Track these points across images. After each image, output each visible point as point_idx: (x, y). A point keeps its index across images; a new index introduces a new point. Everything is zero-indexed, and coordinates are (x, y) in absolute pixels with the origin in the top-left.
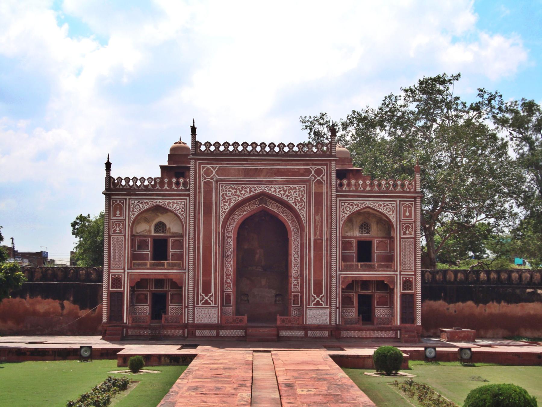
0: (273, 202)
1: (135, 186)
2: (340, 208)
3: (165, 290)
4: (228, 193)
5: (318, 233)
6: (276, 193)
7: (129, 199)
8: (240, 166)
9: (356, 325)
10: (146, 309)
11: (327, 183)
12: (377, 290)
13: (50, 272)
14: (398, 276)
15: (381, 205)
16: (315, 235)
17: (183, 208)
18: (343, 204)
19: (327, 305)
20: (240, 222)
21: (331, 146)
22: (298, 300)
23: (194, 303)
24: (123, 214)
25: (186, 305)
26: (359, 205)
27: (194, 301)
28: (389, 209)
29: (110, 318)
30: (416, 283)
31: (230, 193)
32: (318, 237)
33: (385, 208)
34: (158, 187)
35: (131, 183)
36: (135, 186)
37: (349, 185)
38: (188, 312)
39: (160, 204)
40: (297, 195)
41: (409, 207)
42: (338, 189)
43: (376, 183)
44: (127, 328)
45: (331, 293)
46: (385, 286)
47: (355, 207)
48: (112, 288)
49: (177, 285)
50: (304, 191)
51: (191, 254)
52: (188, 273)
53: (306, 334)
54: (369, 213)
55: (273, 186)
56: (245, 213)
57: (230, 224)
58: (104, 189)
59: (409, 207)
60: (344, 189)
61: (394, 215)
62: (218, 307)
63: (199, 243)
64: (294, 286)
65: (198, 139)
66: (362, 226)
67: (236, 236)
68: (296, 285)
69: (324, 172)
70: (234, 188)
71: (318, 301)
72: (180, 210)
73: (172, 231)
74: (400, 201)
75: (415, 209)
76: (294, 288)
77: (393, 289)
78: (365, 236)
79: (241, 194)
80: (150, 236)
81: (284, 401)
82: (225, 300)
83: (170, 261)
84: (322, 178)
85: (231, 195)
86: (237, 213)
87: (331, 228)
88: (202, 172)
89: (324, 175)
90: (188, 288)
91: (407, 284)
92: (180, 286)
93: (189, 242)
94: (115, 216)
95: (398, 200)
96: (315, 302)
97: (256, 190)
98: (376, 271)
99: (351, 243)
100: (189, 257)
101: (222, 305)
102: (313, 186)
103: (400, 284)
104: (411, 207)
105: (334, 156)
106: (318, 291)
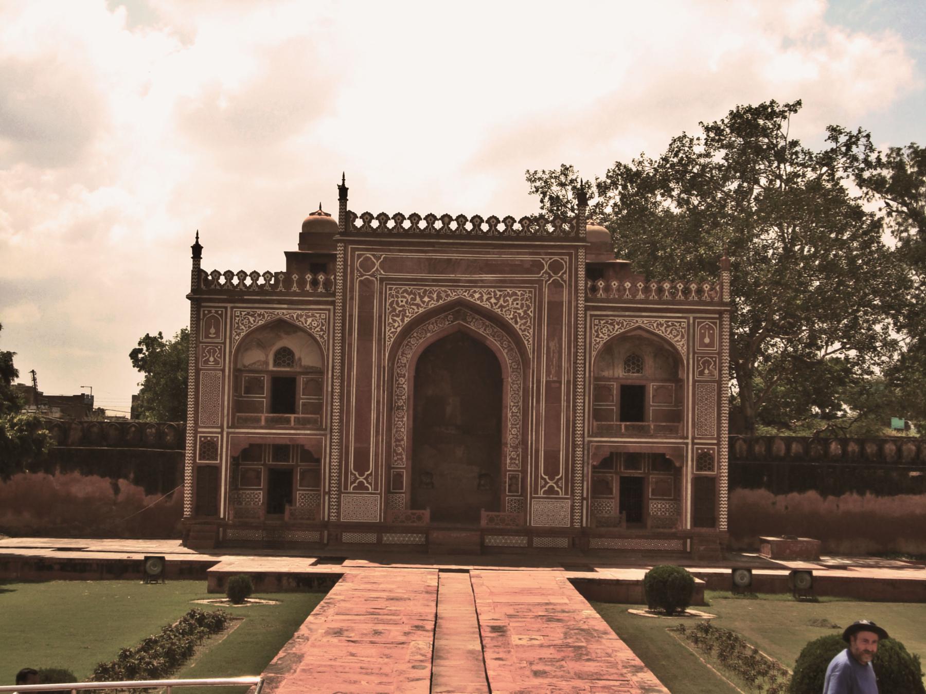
0: (477, 317)
1: (241, 286)
2: (591, 328)
3: (291, 463)
4: (400, 300)
6: (482, 301)
7: (232, 308)
8: (422, 255)
9: (616, 529)
10: (257, 496)
11: (570, 285)
12: (653, 470)
13: (95, 429)
14: (690, 447)
15: (662, 325)
16: (548, 373)
17: (323, 325)
18: (597, 322)
19: (566, 493)
20: (421, 350)
21: (577, 223)
22: (517, 485)
25: (327, 490)
27: (339, 483)
28: (673, 330)
29: (197, 508)
30: (719, 459)
31: (405, 300)
32: (553, 378)
33: (669, 330)
34: (281, 288)
35: (235, 281)
36: (241, 286)
37: (607, 289)
38: (329, 502)
40: (519, 306)
41: (711, 328)
42: (590, 295)
43: (654, 286)
44: (226, 526)
46: (666, 464)
47: (617, 327)
49: (312, 457)
50: (531, 298)
51: (337, 404)
52: (331, 436)
53: (530, 542)
54: (640, 338)
55: (477, 290)
56: (429, 335)
57: (403, 353)
58: (189, 291)
59: (711, 328)
60: (599, 296)
62: (380, 494)
63: (349, 385)
64: (510, 461)
65: (350, 207)
66: (629, 360)
67: (413, 373)
70: (411, 293)
71: (551, 487)
72: (318, 329)
74: (694, 318)
75: (721, 332)
76: (511, 463)
77: (681, 468)
78: (633, 378)
79: (424, 302)
81: (489, 655)
82: (394, 483)
83: (301, 416)
84: (561, 277)
85: (406, 305)
86: (415, 335)
87: (575, 363)
88: (357, 264)
89: (565, 273)
90: (330, 461)
91: (705, 460)
92: (316, 456)
93: (333, 382)
94: (207, 337)
95: (691, 316)
96: (546, 488)
97: (448, 296)
98: (651, 437)
99: (609, 389)
100: (332, 409)
101: (388, 491)
102: (546, 291)
104: (713, 329)
105: (583, 240)
106: (552, 470)
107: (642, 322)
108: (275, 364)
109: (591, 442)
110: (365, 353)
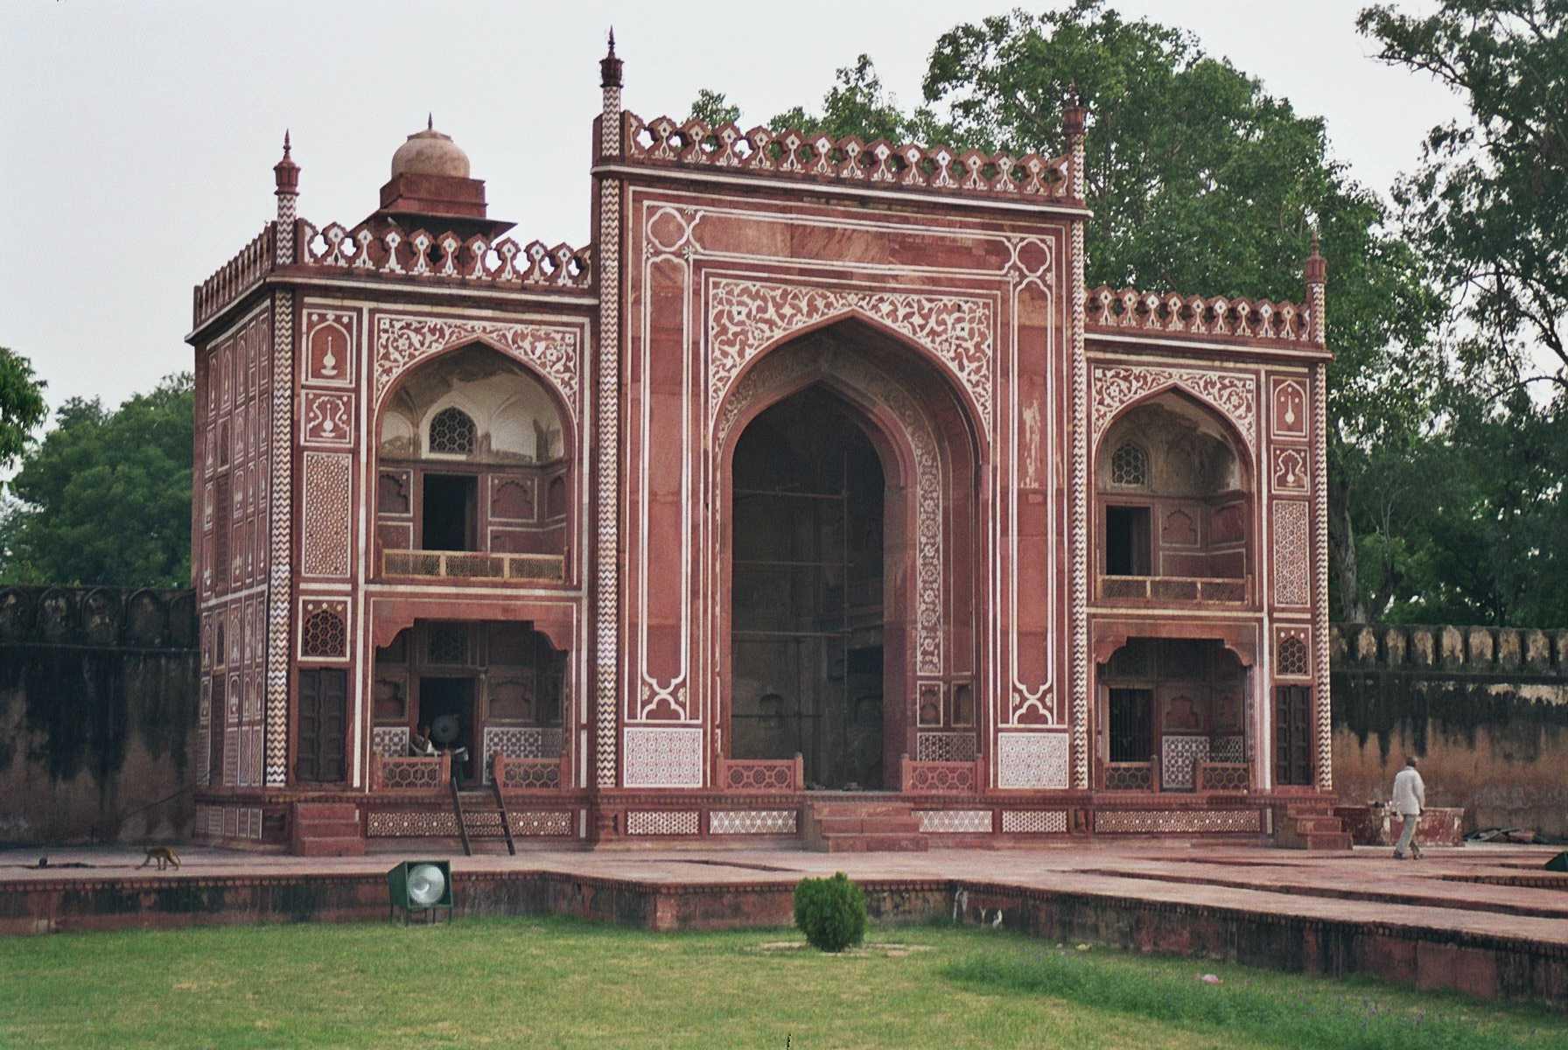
4: (735, 309)
5: (1031, 470)
6: (895, 320)
7: (372, 312)
15: (1213, 385)
17: (569, 359)
18: (1099, 373)
19: (1061, 719)
23: (619, 713)
24: (349, 368)
26: (1149, 379)
27: (619, 705)
30: (1316, 650)
33: (1226, 393)
39: (486, 338)
40: (965, 334)
41: (1296, 394)
45: (1072, 681)
48: (305, 653)
53: (997, 822)
59: (1296, 394)
61: (1251, 417)
66: (1120, 457)
68: (932, 654)
69: (1050, 258)
71: (1033, 708)
73: (494, 447)
74: (1268, 373)
76: (924, 663)
78: (1129, 491)
79: (782, 317)
80: (417, 462)
85: (746, 323)
88: (647, 228)
89: (1049, 270)
91: (1291, 653)
94: (317, 374)
95: (1263, 368)
96: (1023, 711)
98: (1199, 607)
103: (1271, 654)
107: (1183, 376)
108: (432, 449)
109: (1094, 616)
110: (666, 421)
